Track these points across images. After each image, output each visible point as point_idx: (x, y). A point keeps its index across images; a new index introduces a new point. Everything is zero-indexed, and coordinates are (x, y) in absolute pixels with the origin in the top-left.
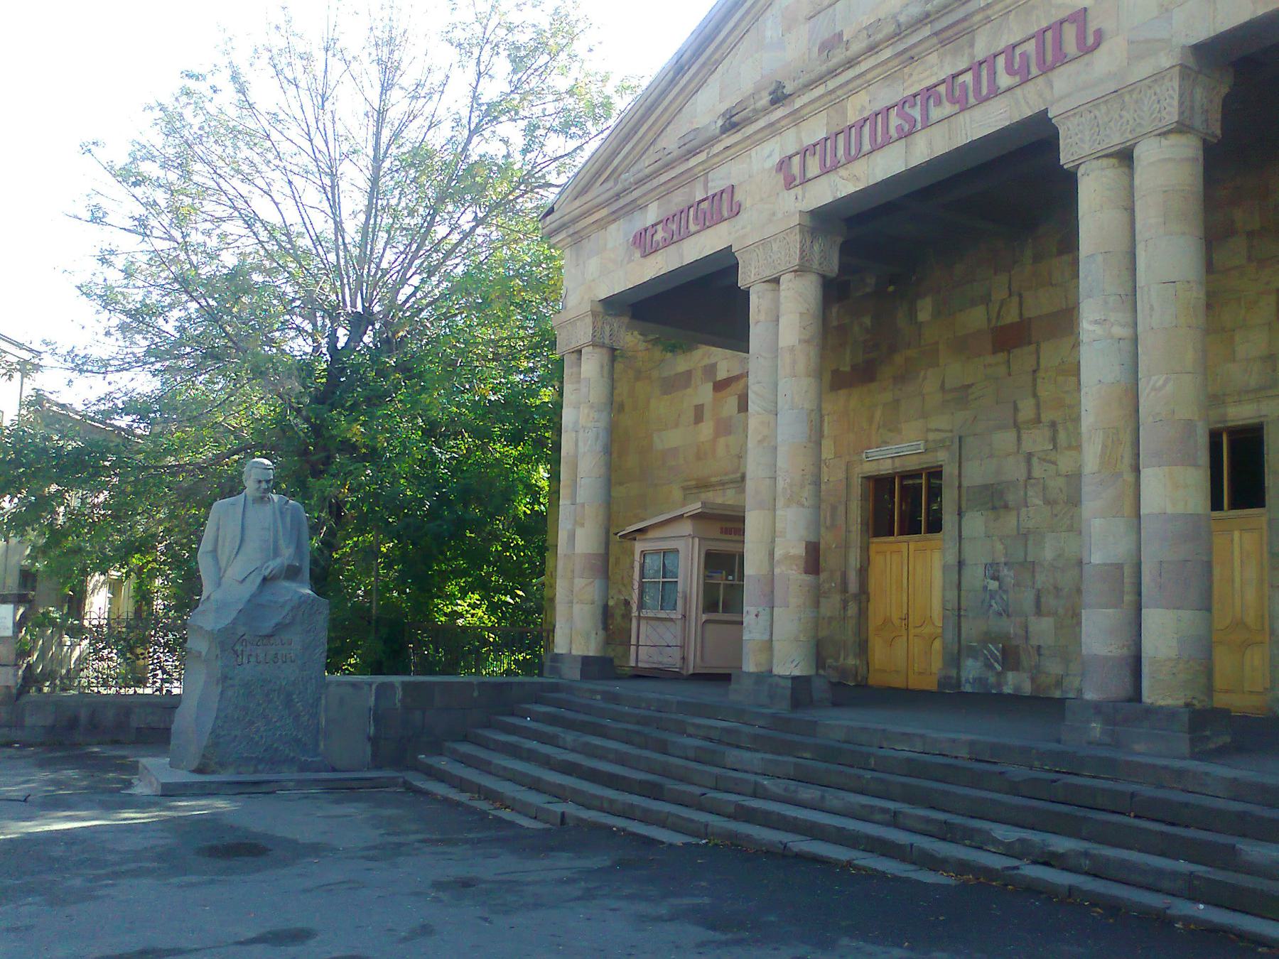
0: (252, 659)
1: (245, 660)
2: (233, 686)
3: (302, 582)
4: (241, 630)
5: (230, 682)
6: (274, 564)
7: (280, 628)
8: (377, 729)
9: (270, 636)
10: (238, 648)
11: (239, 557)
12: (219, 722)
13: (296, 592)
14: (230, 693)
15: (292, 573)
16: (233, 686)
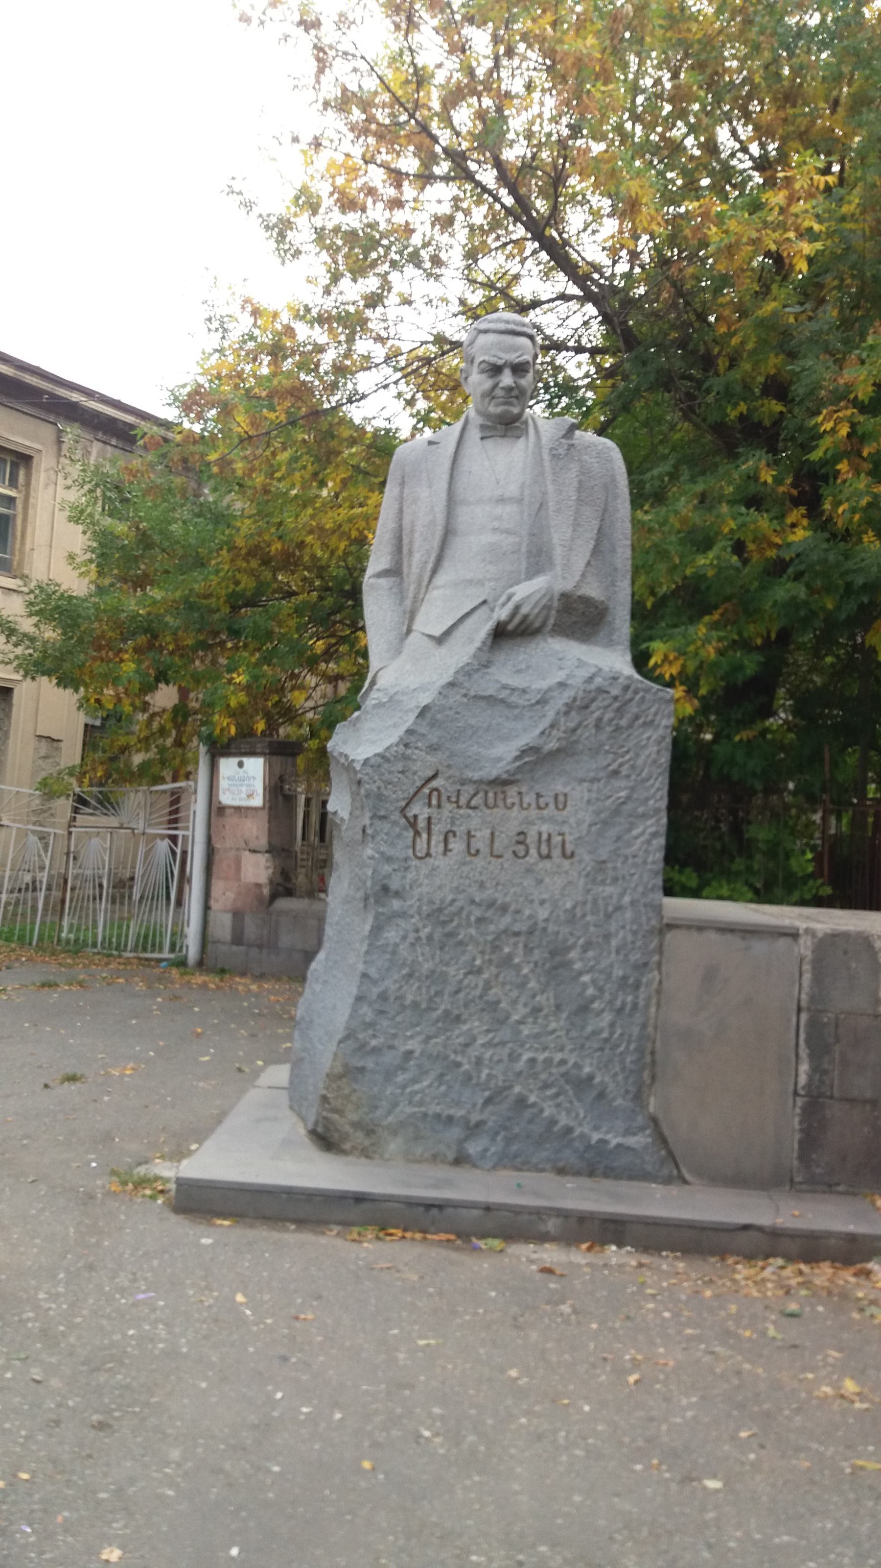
0: (457, 845)
1: (437, 847)
2: (403, 915)
3: (610, 643)
4: (424, 763)
5: (396, 904)
6: (529, 591)
7: (535, 760)
8: (816, 1069)
9: (501, 783)
10: (418, 809)
11: (441, 579)
12: (367, 1012)
13: (581, 664)
14: (391, 935)
15: (577, 617)
16: (403, 915)
